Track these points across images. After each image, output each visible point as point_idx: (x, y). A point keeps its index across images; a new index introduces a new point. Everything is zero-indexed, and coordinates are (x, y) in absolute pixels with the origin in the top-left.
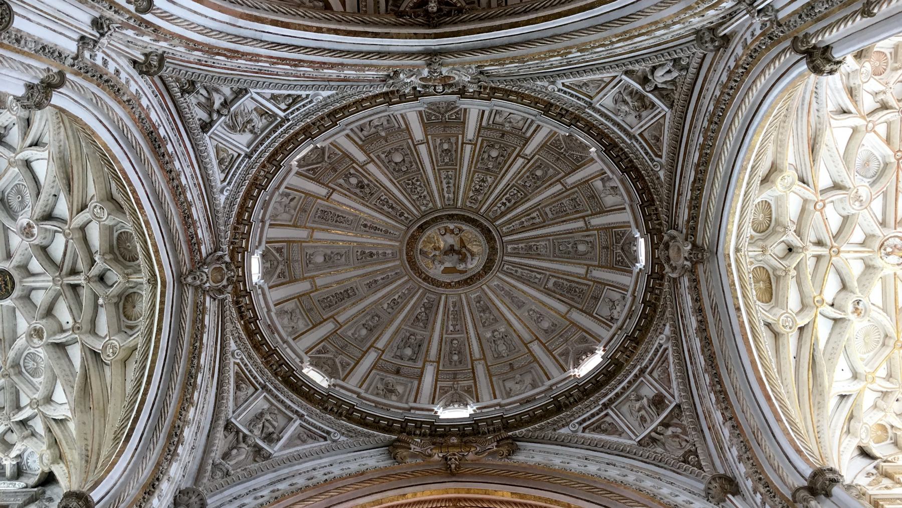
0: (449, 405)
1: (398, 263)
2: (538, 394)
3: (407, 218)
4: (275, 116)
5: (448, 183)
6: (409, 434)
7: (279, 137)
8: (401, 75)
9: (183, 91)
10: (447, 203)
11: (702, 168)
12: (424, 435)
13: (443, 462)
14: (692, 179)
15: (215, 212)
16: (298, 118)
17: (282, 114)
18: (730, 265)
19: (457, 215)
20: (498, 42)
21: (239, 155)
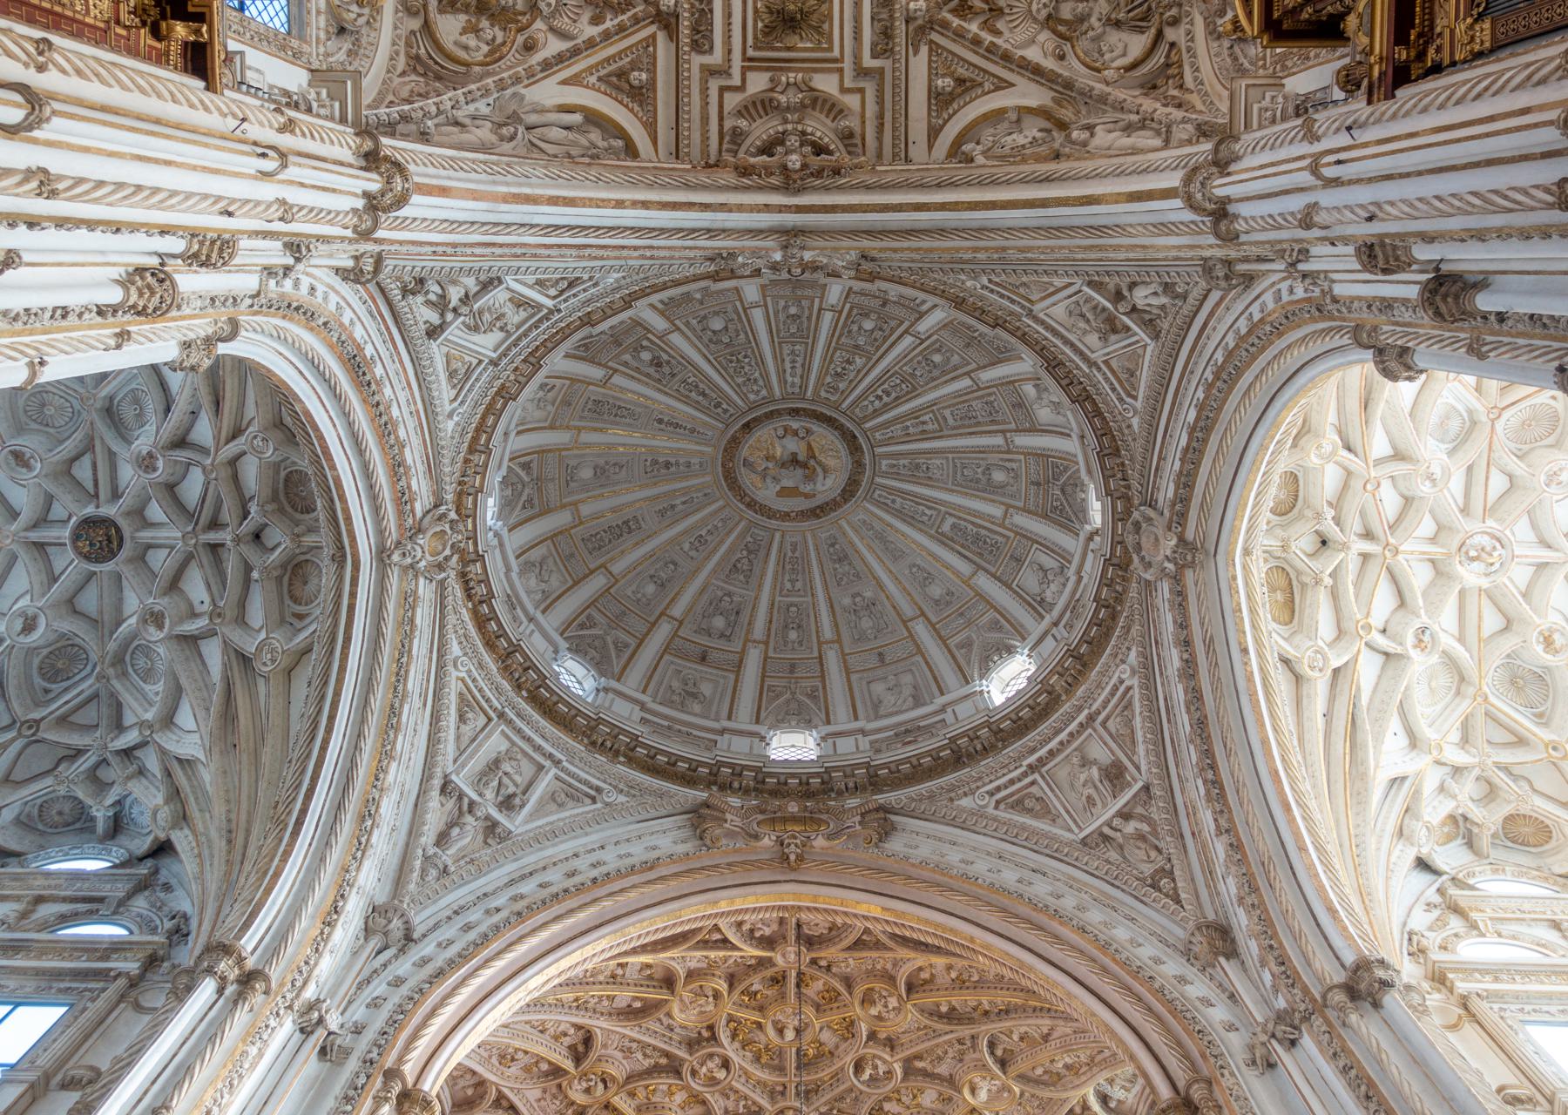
0: (783, 721)
1: (708, 478)
2: (923, 717)
3: (726, 411)
4: (539, 307)
5: (793, 361)
6: (722, 788)
7: (538, 336)
8: (740, 259)
9: (405, 292)
10: (790, 390)
11: (1200, 435)
12: (746, 791)
13: (777, 848)
14: (1184, 442)
15: (437, 450)
16: (572, 305)
17: (549, 303)
18: (1234, 578)
19: (804, 409)
20: (894, 226)
21: (480, 362)
